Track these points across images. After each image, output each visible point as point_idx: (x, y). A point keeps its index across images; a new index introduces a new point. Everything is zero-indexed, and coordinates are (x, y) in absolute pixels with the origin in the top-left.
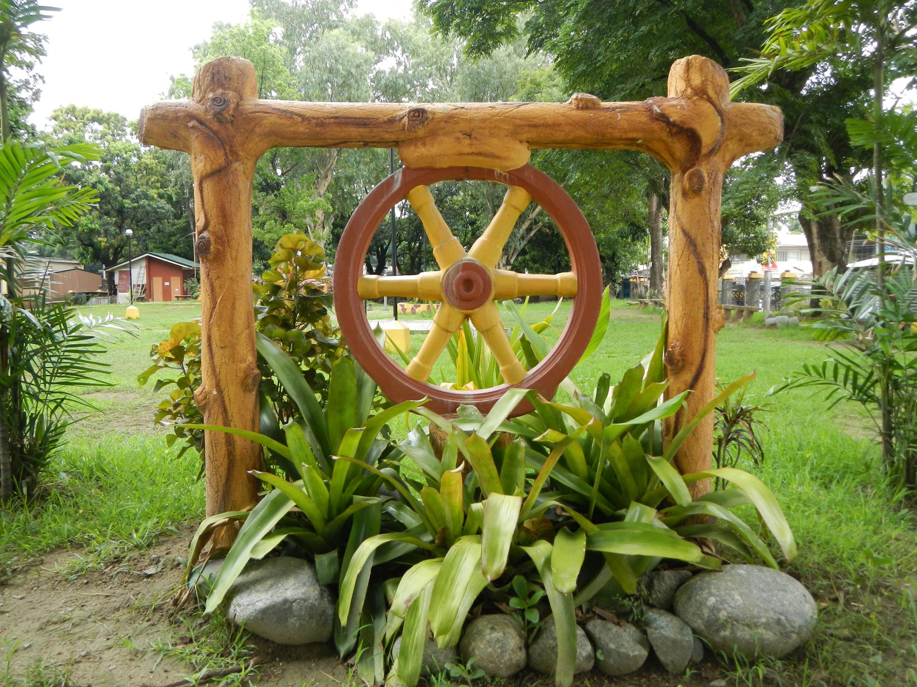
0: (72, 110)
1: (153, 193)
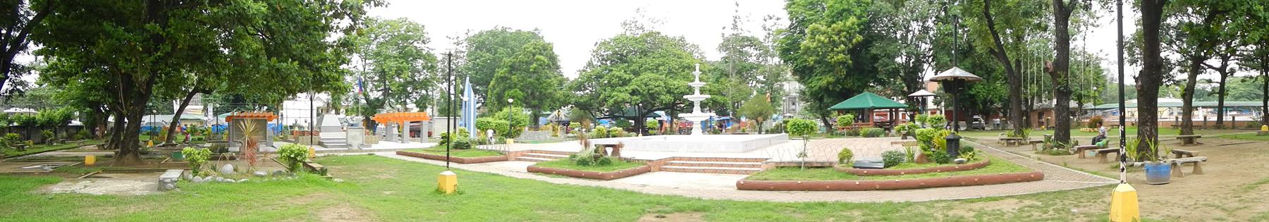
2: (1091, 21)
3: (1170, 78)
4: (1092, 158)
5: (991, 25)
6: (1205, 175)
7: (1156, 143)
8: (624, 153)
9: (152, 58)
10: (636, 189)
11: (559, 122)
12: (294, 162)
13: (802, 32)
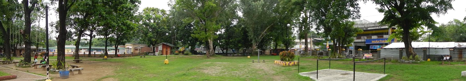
1: (166, 27)
2: (42, 15)
3: (72, 38)
4: (40, 68)
6: (83, 75)
7: (64, 62)
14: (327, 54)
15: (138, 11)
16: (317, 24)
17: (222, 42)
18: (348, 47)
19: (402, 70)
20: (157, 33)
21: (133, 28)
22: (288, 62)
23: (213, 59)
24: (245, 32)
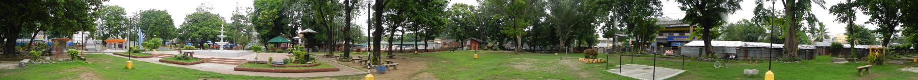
0: (456, 4)
1: (474, 23)
2: (358, 13)
5: (322, 13)
8: (194, 56)
9: (21, 17)
10: (198, 69)
11: (173, 44)
12: (73, 56)
13: (259, 14)
14: (630, 51)
15: (447, 7)
16: (620, 21)
17: (529, 39)
18: (650, 43)
19: (701, 67)
20: (465, 28)
21: (444, 23)
22: (592, 60)
23: (521, 55)
24: (553, 30)
